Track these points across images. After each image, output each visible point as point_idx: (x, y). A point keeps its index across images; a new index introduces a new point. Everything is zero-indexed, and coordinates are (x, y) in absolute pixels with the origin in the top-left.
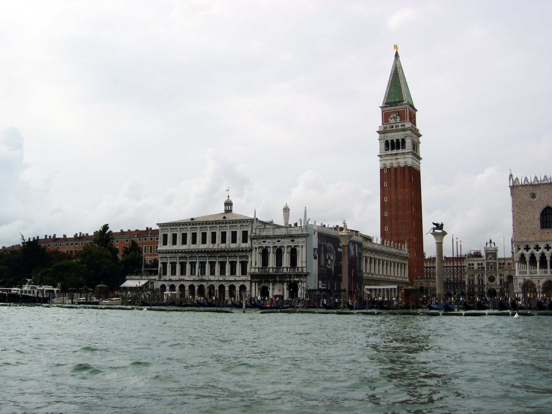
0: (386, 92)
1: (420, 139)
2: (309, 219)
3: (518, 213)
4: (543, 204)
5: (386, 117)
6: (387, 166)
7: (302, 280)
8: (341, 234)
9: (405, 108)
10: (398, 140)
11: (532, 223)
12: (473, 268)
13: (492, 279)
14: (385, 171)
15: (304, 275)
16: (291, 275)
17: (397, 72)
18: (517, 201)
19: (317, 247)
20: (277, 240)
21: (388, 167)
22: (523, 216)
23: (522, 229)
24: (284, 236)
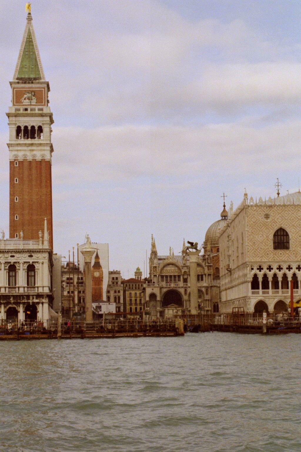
3: (252, 233)
4: (277, 225)
5: (18, 97)
6: (19, 158)
9: (43, 88)
10: (33, 127)
11: (265, 244)
14: (16, 164)
16: (30, 295)
17: (31, 40)
18: (252, 221)
20: (10, 255)
21: (20, 159)
22: (256, 237)
23: (256, 250)
24: (20, 251)
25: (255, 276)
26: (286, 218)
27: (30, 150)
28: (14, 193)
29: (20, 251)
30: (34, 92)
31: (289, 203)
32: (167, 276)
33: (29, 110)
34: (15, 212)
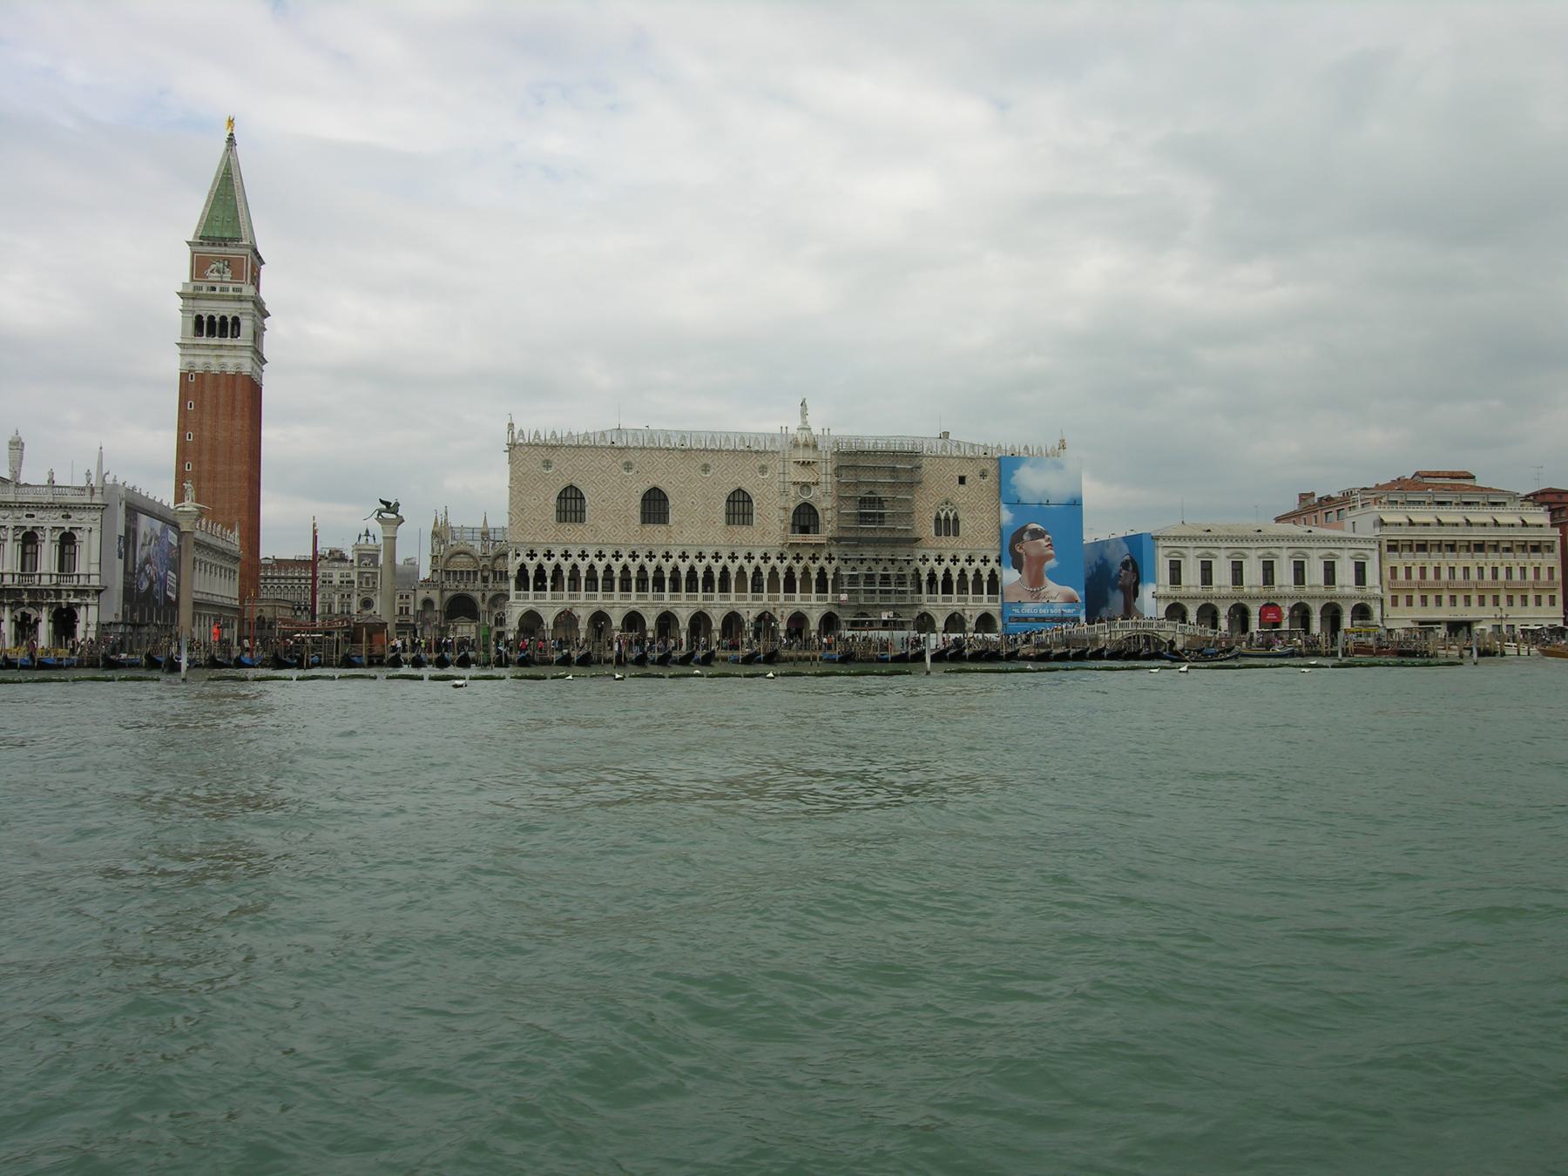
0: (203, 213)
1: (266, 321)
2: (107, 474)
5: (199, 266)
6: (197, 368)
7: (89, 601)
10: (223, 318)
12: (331, 582)
15: (94, 592)
16: (61, 590)
19: (123, 535)
20: (26, 513)
21: (199, 369)
22: (527, 499)
24: (45, 506)
25: (523, 569)
26: (581, 468)
27: (216, 356)
28: (185, 426)
29: (45, 506)
31: (586, 443)
32: (455, 572)
33: (218, 289)
34: (187, 458)
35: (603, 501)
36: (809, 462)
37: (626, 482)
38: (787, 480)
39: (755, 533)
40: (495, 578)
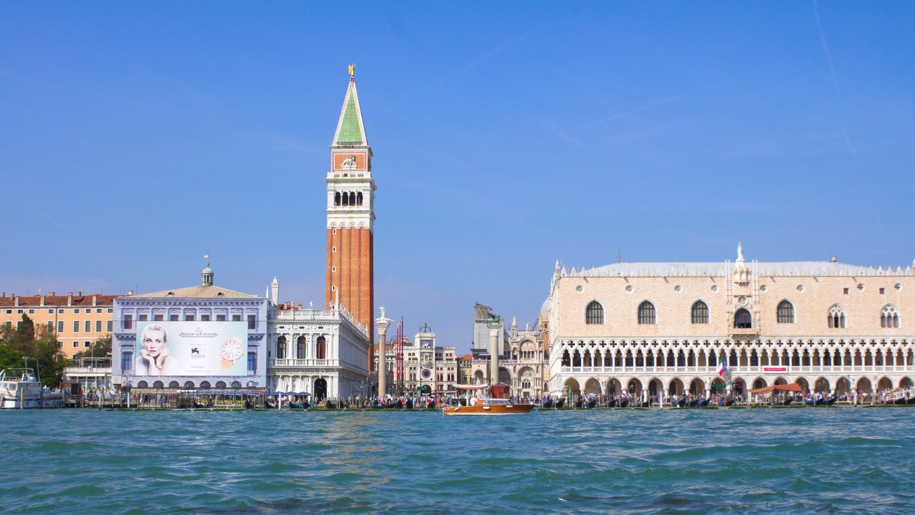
1: (374, 192)
3: (564, 306)
8: (378, 322)
9: (364, 153)
10: (352, 193)
13: (426, 374)
17: (353, 103)
20: (299, 326)
21: (338, 226)
25: (566, 354)
26: (601, 290)
27: (349, 217)
28: (331, 263)
30: (355, 158)
31: (604, 275)
33: (349, 175)
35: (615, 310)
36: (744, 283)
37: (629, 298)
38: (730, 294)
39: (711, 329)
40: (521, 357)
